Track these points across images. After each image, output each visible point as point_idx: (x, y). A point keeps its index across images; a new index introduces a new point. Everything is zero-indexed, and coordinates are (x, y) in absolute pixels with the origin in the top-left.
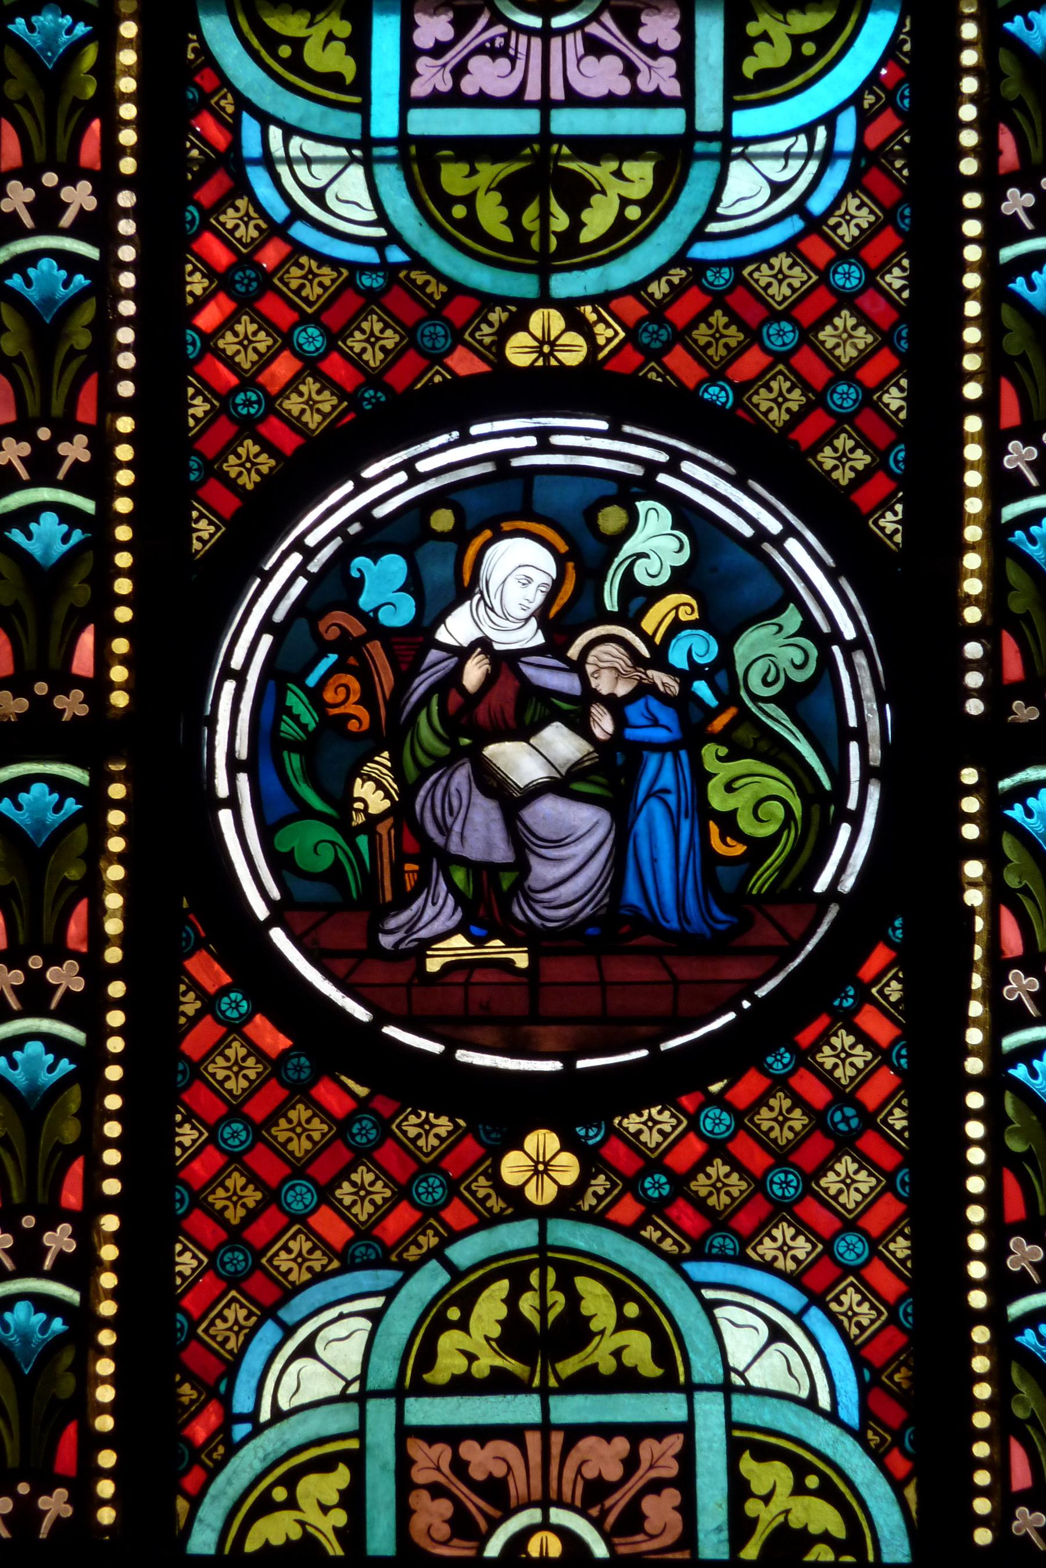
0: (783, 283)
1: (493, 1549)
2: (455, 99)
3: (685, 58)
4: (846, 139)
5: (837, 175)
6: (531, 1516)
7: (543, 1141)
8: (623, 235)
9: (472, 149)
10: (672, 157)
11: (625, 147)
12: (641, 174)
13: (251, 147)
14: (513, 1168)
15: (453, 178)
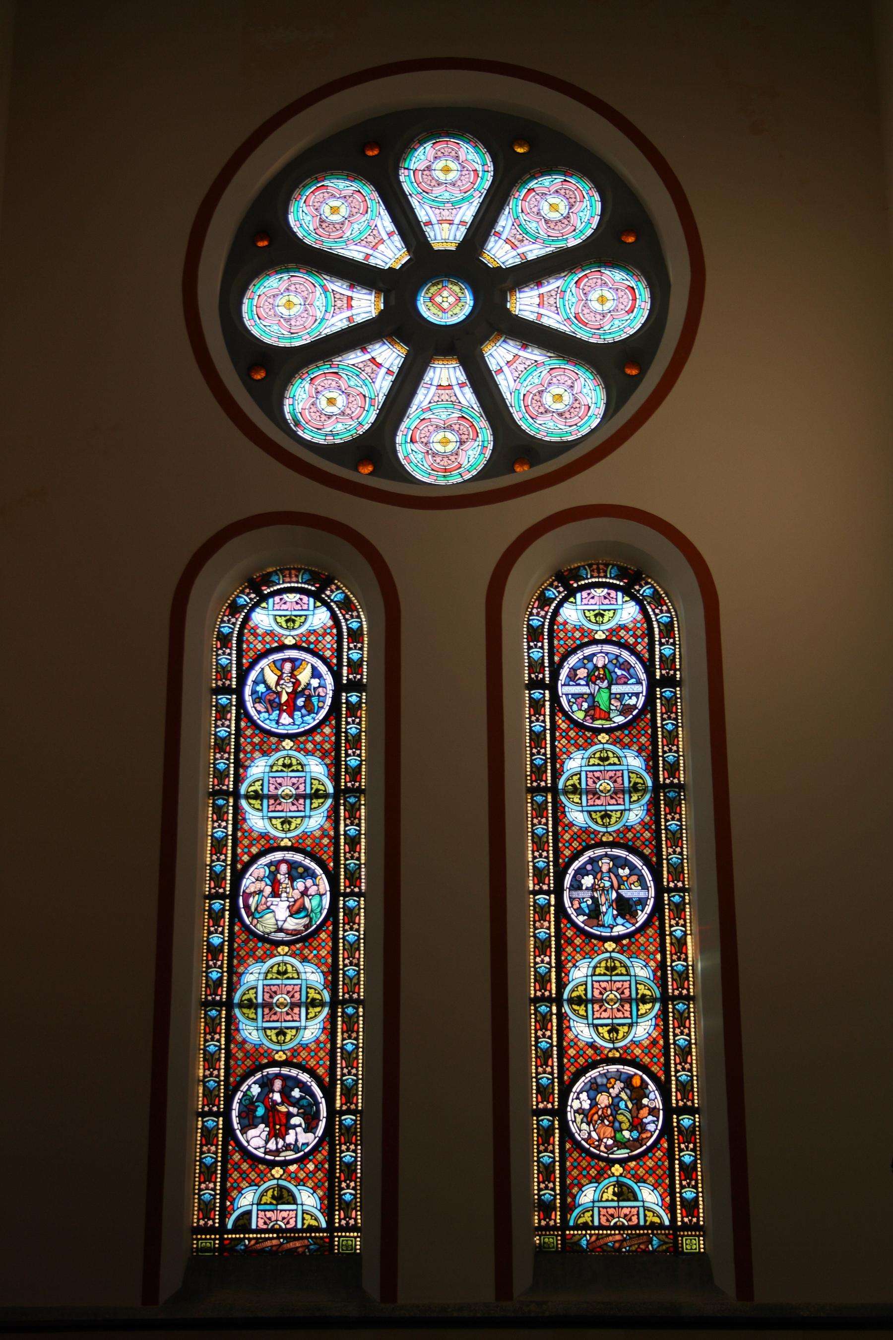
0: (646, 1043)
1: (612, 1224)
2: (600, 1018)
3: (631, 1012)
4: (653, 1023)
5: (652, 1027)
6: (617, 1220)
7: (617, 1166)
8: (624, 1037)
9: (602, 1025)
10: (630, 1026)
11: (624, 1025)
12: (626, 1029)
13: (572, 1024)
14: (613, 1169)
15: (600, 1029)
